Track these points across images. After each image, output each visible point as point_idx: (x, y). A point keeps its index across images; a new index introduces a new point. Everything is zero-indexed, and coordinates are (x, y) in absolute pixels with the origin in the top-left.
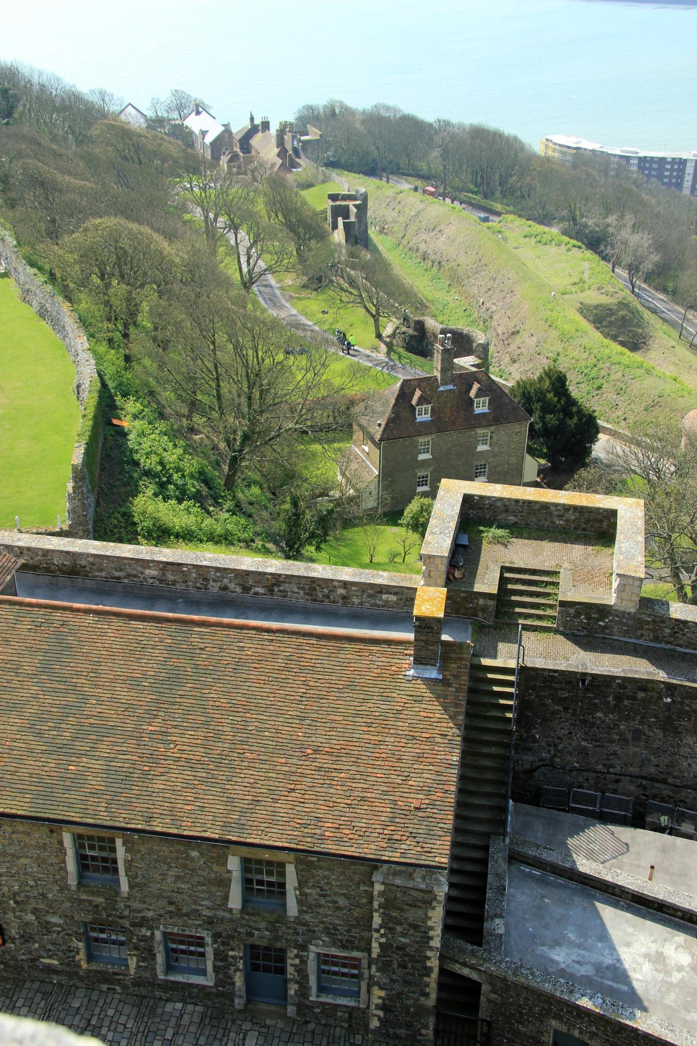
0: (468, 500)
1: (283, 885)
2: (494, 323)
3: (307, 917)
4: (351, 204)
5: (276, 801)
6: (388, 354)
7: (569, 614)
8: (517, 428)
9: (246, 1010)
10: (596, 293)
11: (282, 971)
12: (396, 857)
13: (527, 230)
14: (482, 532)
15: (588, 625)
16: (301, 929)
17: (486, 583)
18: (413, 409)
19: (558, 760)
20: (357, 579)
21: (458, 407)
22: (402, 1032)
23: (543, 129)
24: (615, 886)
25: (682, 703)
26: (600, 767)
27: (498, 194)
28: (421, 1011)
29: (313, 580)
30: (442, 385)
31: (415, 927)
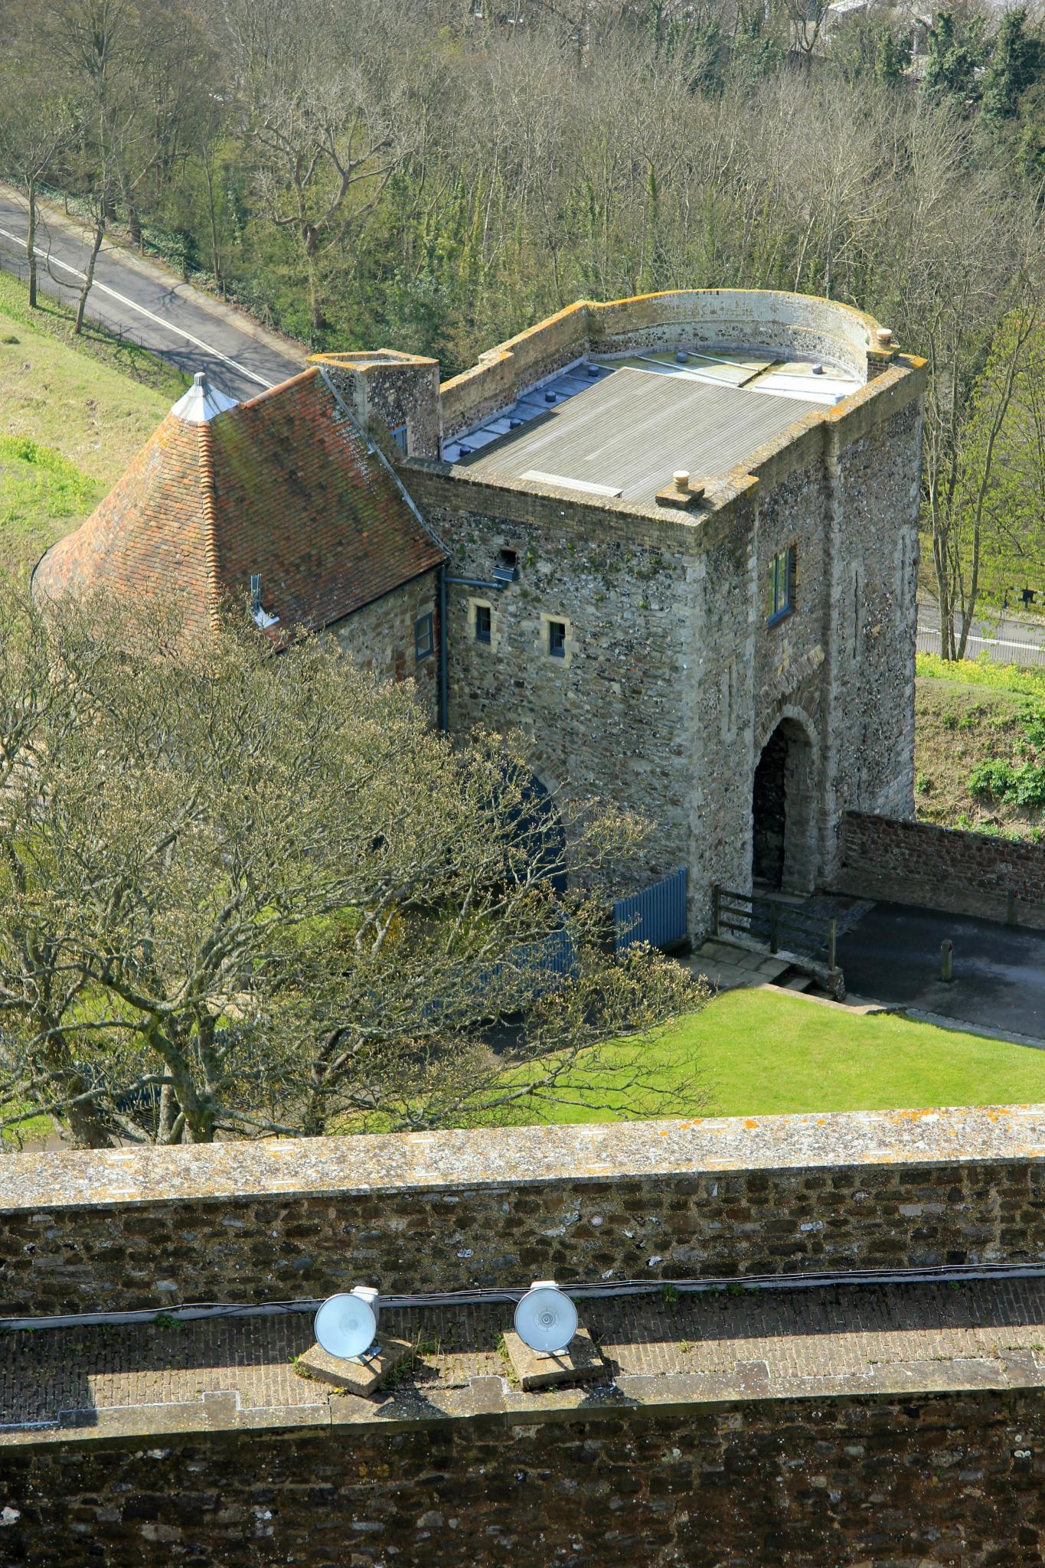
25: (58, 1513)
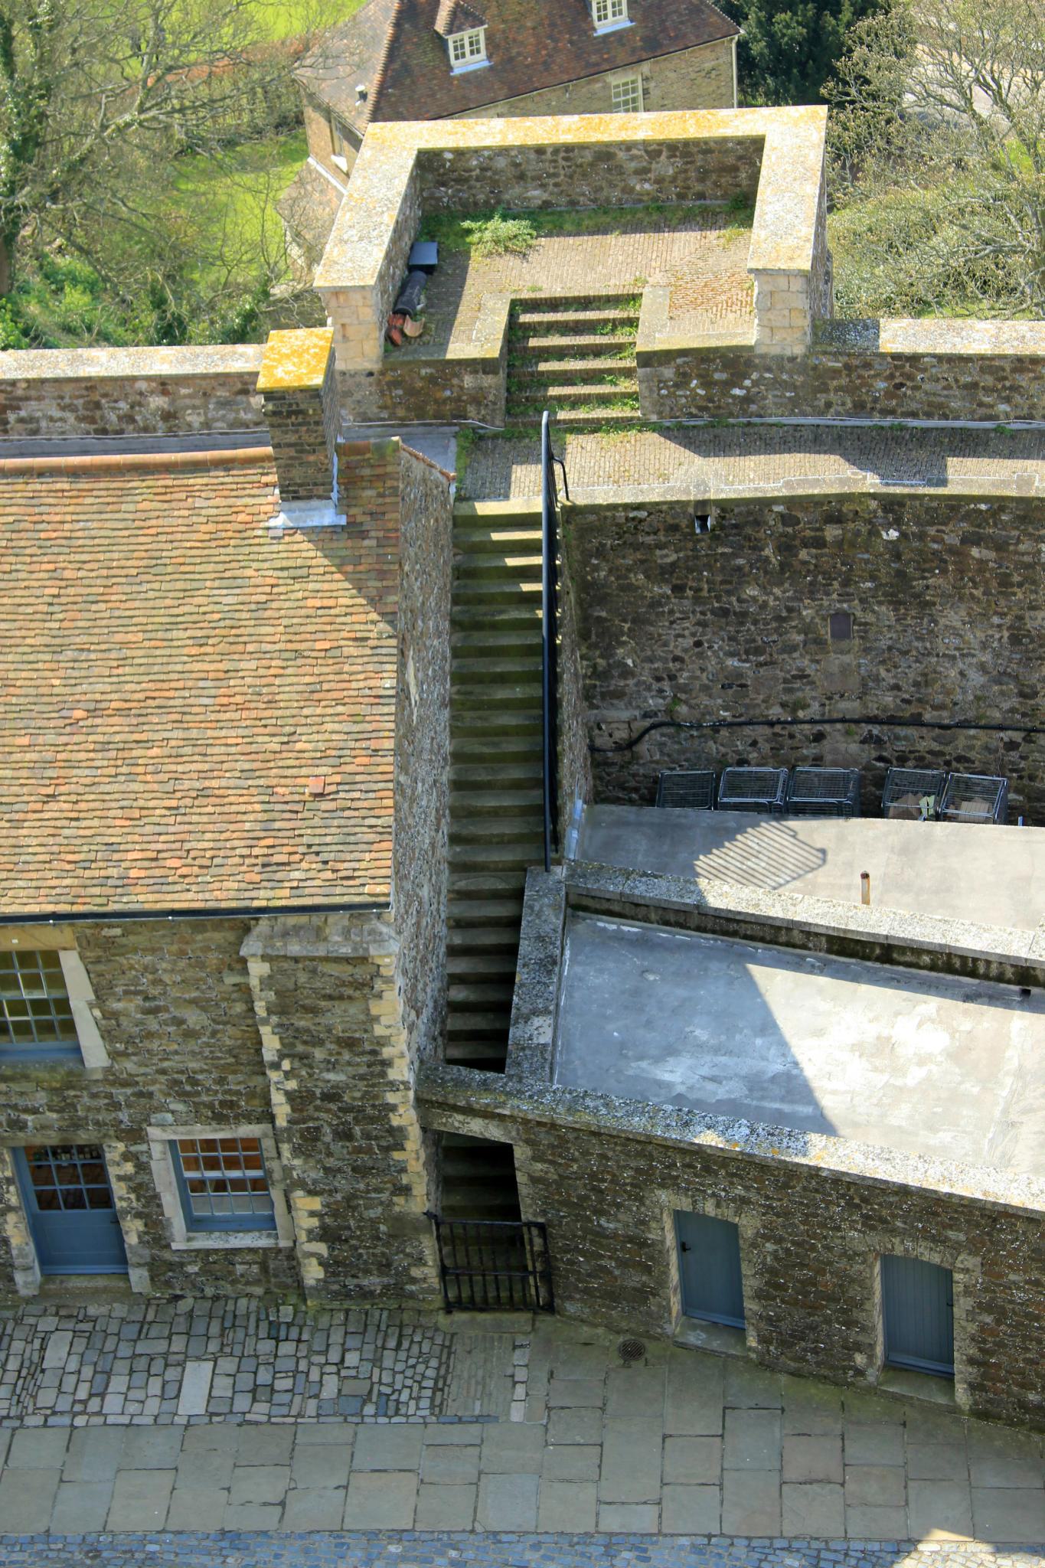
0: (427, 163)
1: (63, 1005)
3: (130, 1066)
5: (17, 824)
7: (662, 382)
9: (43, 1295)
11: (104, 1199)
12: (282, 897)
14: (469, 232)
15: (708, 396)
16: (121, 1094)
18: (441, 43)
19: (683, 709)
20: (187, 369)
21: (553, 25)
22: (373, 1282)
24: (790, 926)
26: (775, 712)
28: (402, 1228)
29: (90, 385)
31: (350, 1044)
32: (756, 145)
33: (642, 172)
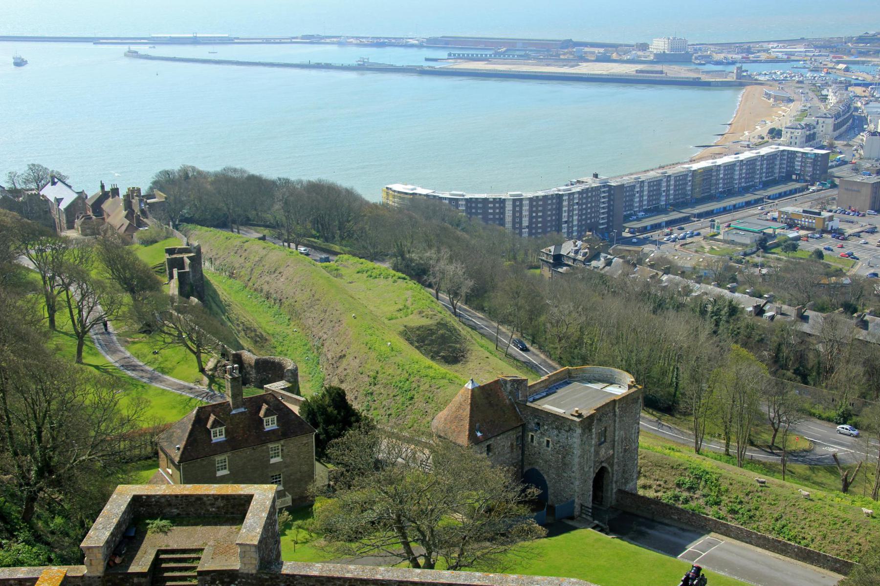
0: (136, 499)
2: (325, 350)
4: (185, 256)
6: (210, 386)
8: (304, 439)
10: (418, 316)
13: (360, 267)
14: (148, 524)
17: (141, 564)
23: (376, 182)
27: (337, 237)
30: (234, 408)
32: (250, 498)
33: (212, 505)
